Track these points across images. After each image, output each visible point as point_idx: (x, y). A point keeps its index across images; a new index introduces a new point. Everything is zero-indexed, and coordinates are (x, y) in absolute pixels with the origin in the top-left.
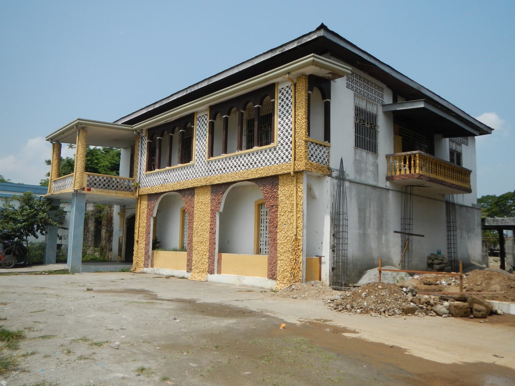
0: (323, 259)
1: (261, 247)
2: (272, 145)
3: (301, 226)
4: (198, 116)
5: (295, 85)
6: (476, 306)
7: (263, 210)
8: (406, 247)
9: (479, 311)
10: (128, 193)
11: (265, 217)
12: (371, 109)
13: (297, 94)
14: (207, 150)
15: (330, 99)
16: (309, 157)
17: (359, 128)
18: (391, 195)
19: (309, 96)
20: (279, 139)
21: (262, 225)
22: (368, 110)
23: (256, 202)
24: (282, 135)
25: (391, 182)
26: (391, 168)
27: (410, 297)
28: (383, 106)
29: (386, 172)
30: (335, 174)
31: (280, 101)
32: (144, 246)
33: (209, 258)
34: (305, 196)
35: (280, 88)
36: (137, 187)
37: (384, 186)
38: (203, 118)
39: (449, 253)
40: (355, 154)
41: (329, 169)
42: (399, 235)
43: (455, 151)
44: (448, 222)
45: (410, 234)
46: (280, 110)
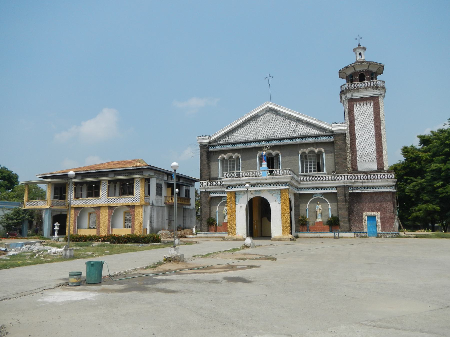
0: (147, 229)
1: (126, 226)
2: (133, 196)
3: (142, 220)
4: (102, 182)
5: (141, 180)
6: (183, 236)
7: (126, 214)
8: (169, 224)
9: (183, 237)
10: (64, 207)
11: (127, 216)
12: (161, 182)
13: (142, 183)
14: (107, 194)
15: (150, 182)
16: (145, 200)
17: (157, 190)
18: (166, 208)
19: (145, 184)
20: (136, 195)
21: (126, 219)
22: (160, 183)
23: (124, 212)
24: (136, 194)
25: (166, 204)
26: (166, 200)
27: (170, 235)
28: (164, 180)
29: (164, 201)
30: (151, 205)
31: (136, 183)
32: (73, 228)
33: (108, 230)
34: (143, 211)
35: (136, 180)
36: (69, 204)
37: (164, 206)
38: (105, 183)
39: (183, 225)
40: (156, 197)
41: (149, 203)
42: (168, 220)
43: (187, 189)
44: (184, 215)
45: (170, 220)
46: (136, 186)
